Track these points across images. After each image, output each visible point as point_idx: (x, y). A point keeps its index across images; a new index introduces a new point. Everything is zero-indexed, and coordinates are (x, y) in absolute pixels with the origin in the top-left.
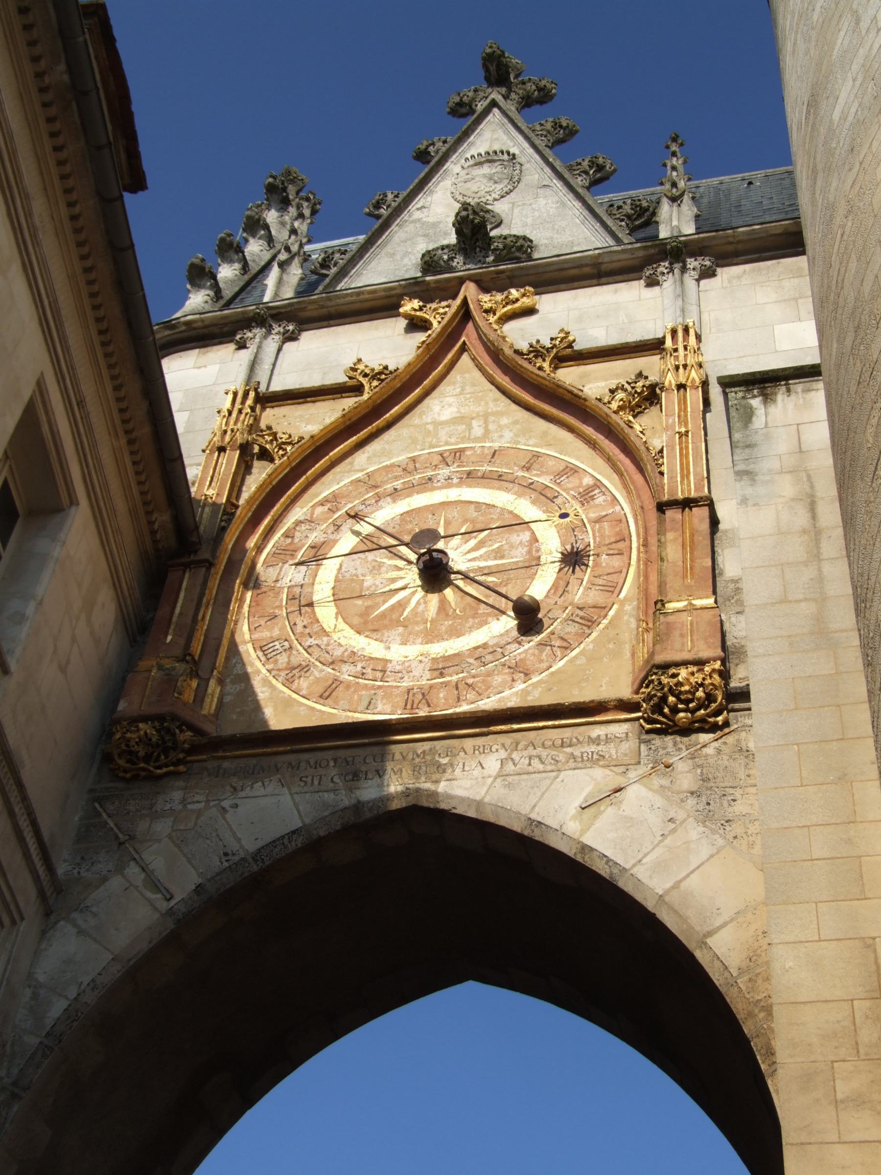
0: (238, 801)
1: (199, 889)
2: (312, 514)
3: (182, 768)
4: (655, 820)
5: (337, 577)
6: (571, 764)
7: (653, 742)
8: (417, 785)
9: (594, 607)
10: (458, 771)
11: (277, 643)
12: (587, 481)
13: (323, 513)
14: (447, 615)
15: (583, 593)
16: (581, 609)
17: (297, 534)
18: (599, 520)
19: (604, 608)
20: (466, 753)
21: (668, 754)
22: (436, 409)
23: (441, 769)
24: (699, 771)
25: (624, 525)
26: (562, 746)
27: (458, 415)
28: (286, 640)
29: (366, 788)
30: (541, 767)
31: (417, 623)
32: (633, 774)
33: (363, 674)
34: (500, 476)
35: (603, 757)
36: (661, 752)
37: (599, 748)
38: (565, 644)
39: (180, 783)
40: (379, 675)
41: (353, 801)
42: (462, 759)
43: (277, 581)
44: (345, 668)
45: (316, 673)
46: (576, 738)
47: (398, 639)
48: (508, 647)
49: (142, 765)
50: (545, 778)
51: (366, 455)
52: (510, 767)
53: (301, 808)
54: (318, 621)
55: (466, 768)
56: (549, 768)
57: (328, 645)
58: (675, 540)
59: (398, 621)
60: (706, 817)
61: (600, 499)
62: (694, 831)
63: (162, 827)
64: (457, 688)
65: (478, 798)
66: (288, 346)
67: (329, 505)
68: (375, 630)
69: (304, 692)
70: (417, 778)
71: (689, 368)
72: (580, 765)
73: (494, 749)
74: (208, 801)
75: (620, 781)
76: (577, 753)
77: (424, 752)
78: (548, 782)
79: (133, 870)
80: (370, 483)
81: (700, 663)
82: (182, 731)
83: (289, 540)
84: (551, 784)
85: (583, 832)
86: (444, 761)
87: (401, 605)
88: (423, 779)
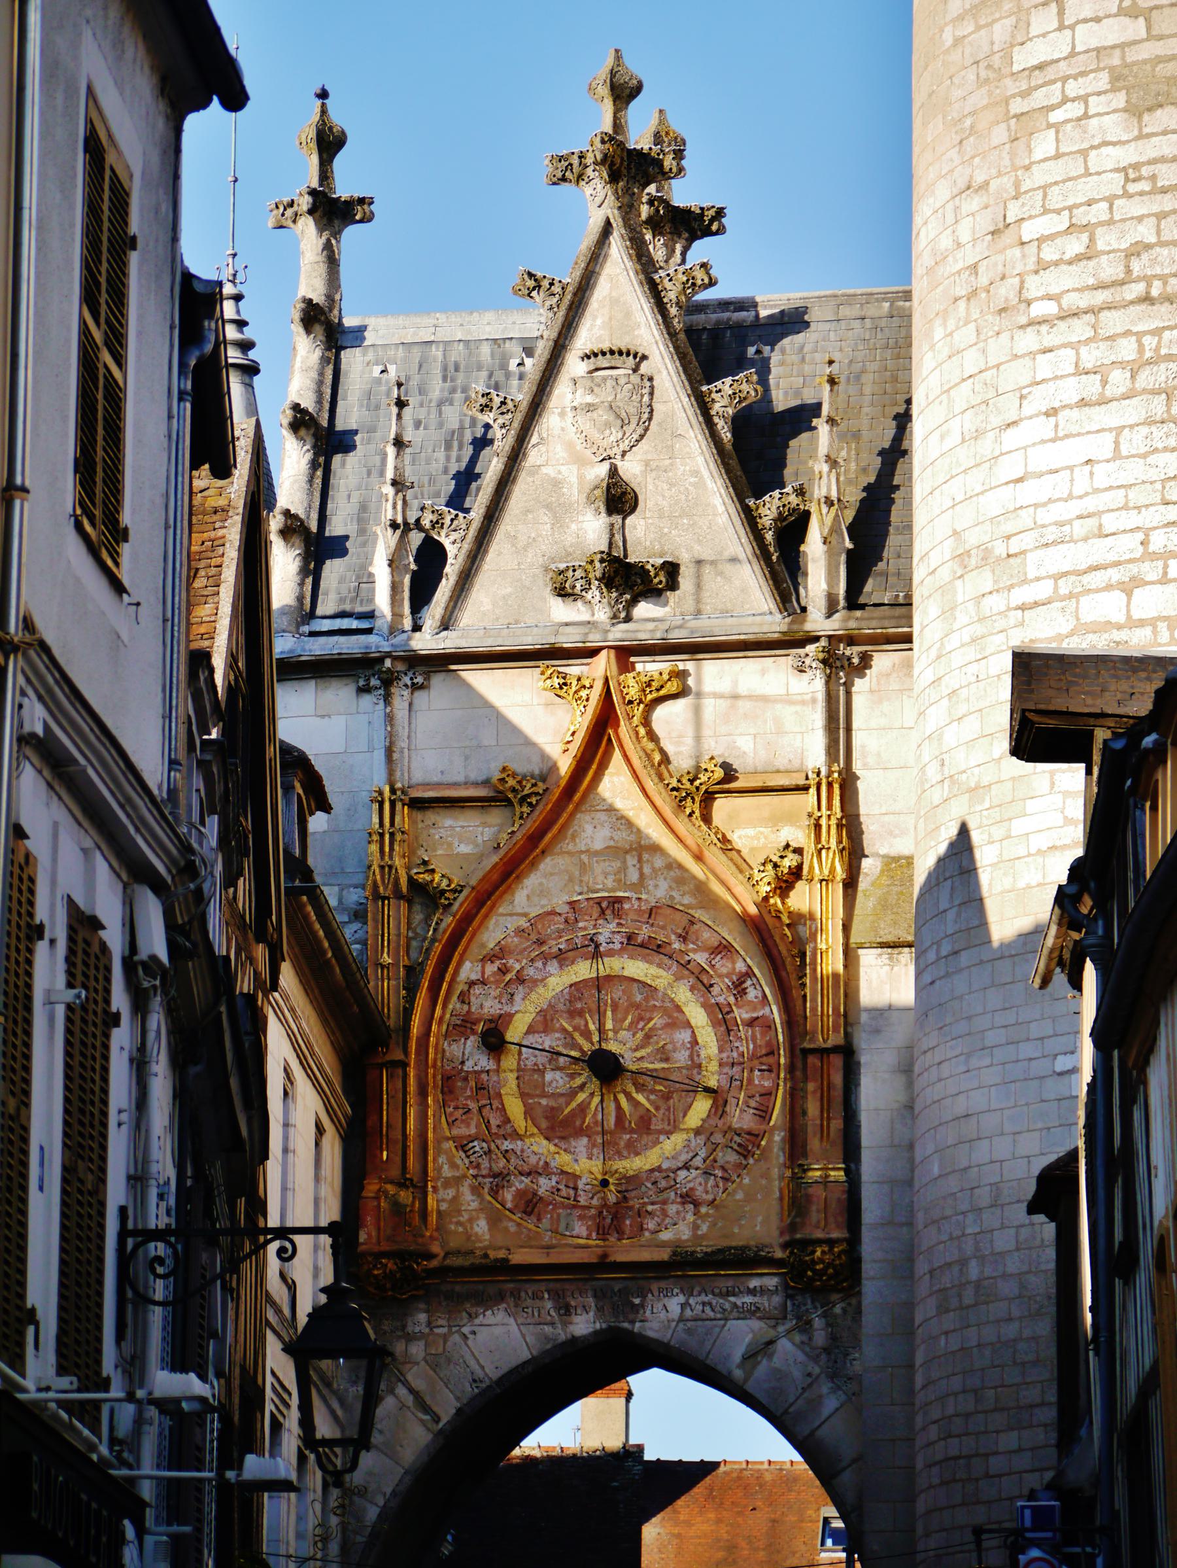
1: (459, 1411)
2: (483, 973)
3: (421, 1292)
4: (797, 1373)
6: (735, 1314)
9: (749, 1133)
10: (648, 1312)
12: (740, 966)
13: (494, 974)
15: (740, 1117)
17: (473, 999)
18: (751, 1023)
22: (589, 829)
23: (635, 1309)
27: (612, 843)
30: (712, 1314)
32: (781, 1329)
34: (659, 946)
37: (756, 1299)
39: (422, 1306)
40: (572, 1192)
43: (463, 1063)
44: (542, 1181)
58: (814, 1092)
59: (581, 1129)
60: (835, 1374)
61: (752, 994)
62: (825, 1387)
63: (417, 1350)
66: (417, 694)
67: (498, 963)
68: (562, 1138)
69: (509, 1205)
75: (772, 1333)
76: (739, 1303)
79: (401, 1391)
80: (534, 934)
81: (831, 1243)
83: (466, 1007)
85: (746, 1380)
86: (637, 1301)
87: (583, 1108)
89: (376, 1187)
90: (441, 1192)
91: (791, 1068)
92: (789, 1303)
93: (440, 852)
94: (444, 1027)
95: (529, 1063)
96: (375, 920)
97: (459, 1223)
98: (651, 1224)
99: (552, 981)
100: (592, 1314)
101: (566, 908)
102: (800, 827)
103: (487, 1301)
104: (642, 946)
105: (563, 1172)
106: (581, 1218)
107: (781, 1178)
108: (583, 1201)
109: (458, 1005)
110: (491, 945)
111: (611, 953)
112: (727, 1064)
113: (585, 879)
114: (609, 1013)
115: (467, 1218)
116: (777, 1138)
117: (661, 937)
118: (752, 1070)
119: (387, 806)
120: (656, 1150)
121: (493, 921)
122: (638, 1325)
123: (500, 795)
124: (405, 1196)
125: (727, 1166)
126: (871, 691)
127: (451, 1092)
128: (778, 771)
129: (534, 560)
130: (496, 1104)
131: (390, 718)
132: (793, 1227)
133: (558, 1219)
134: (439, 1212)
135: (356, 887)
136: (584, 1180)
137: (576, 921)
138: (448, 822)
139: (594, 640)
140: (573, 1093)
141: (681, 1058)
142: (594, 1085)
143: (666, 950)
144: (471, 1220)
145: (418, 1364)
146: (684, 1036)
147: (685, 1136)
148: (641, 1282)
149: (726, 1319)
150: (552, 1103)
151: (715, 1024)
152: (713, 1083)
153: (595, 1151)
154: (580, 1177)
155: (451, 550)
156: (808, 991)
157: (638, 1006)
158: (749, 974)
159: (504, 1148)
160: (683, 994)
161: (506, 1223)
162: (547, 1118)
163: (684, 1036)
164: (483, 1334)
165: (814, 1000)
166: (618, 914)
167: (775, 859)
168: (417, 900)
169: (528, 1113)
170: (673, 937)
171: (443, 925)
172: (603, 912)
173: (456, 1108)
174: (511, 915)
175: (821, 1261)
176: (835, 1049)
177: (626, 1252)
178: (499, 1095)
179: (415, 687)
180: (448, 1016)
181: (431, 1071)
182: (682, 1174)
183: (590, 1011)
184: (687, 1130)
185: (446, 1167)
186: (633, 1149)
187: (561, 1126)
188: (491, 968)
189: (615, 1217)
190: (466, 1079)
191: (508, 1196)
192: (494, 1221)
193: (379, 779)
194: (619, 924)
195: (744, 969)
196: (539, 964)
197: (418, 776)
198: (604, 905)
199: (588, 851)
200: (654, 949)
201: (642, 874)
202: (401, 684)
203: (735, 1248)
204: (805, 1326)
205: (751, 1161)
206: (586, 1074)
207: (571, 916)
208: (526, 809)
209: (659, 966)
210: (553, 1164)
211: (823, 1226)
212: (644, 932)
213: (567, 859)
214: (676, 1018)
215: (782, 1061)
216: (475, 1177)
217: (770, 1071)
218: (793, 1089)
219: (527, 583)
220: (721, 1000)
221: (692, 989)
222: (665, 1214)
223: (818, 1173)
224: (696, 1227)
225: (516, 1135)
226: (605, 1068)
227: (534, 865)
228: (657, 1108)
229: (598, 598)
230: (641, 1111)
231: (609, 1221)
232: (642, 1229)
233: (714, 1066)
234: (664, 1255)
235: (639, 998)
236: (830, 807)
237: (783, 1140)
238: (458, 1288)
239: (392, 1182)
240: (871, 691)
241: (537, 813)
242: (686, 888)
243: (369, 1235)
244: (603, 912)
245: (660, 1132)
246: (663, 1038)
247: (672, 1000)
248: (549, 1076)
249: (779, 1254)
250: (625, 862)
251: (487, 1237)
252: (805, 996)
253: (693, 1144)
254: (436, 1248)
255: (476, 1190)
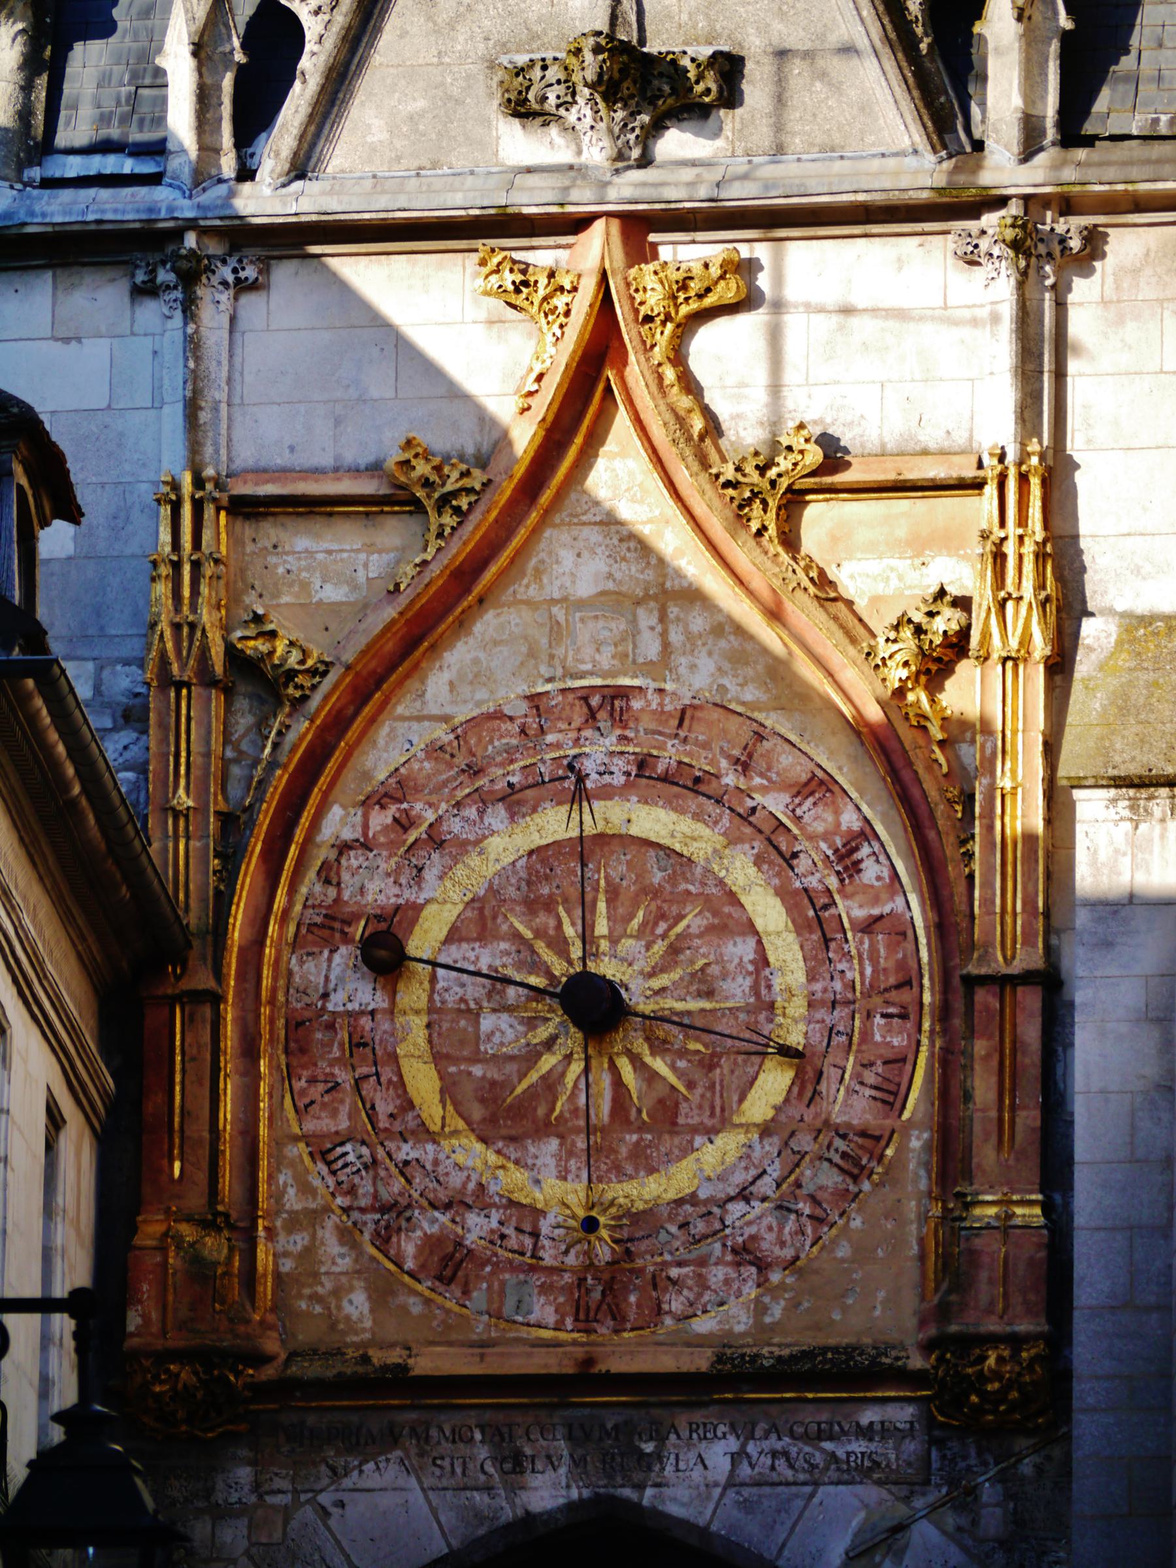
0: (346, 1497)
2: (366, 826)
5: (431, 999)
6: (833, 1474)
7: (950, 1444)
8: (612, 1490)
9: (863, 1134)
10: (669, 1469)
11: (348, 1147)
12: (850, 820)
13: (386, 829)
14: (628, 1122)
16: (844, 1137)
17: (346, 876)
18: (869, 926)
19: (878, 1139)
20: (679, 1437)
21: (969, 1468)
22: (567, 558)
23: (646, 1462)
24: (1011, 1505)
25: (910, 946)
26: (820, 1439)
27: (610, 586)
28: (363, 1143)
29: (536, 1489)
30: (789, 1474)
31: (577, 1131)
32: (919, 1503)
33: (503, 1237)
34: (697, 780)
35: (878, 1464)
36: (962, 1465)
37: (873, 1446)
38: (818, 1212)
39: (244, 1453)
40: (528, 1242)
41: (520, 1512)
42: (675, 1446)
43: (325, 996)
44: (473, 1219)
45: (425, 1225)
46: (839, 1424)
47: (552, 1162)
48: (729, 1206)
49: (184, 1428)
50: (797, 1496)
51: (446, 676)
52: (745, 1471)
53: (443, 1519)
54: (410, 1105)
55: (682, 1466)
56: (802, 1477)
57: (436, 1162)
58: (987, 1058)
59: (548, 1124)
61: (871, 872)
63: (234, 1535)
64: (655, 1287)
65: (701, 1522)
66: (246, 299)
67: (393, 809)
68: (513, 1139)
69: (410, 1264)
70: (611, 1477)
71: (1024, 606)
72: (846, 1477)
73: (719, 1434)
74: (296, 1492)
75: (902, 1511)
76: (841, 1453)
77: (616, 1427)
78: (800, 1503)
80: (463, 753)
81: (1016, 1341)
82: (238, 1374)
83: (332, 892)
84: (805, 1507)
86: (649, 1447)
87: (550, 1083)
88: (619, 1480)
89: (160, 1228)
90: (282, 1238)
91: (944, 1013)
92: (934, 1454)
93: (285, 599)
94: (292, 929)
95: (451, 999)
96: (163, 726)
97: (315, 1298)
98: (676, 1304)
99: (495, 844)
100: (563, 1470)
101: (523, 707)
102: (965, 557)
103: (368, 1444)
104: (665, 779)
105: (512, 1203)
106: (544, 1289)
107: (923, 1218)
108: (549, 1257)
109: (318, 888)
110: (382, 776)
111: (607, 793)
112: (823, 1003)
113: (560, 651)
114: (602, 906)
115: (332, 1287)
116: (915, 1144)
117: (702, 764)
118: (869, 1015)
119: (187, 511)
120: (688, 1163)
121: (384, 731)
122: (649, 1492)
123: (399, 496)
124: (214, 1246)
125: (820, 1195)
126: (1104, 302)
127: (303, 1051)
128: (925, 452)
129: (468, 45)
130: (387, 1073)
131: (193, 345)
132: (943, 1312)
133: (502, 1293)
134: (278, 1276)
135: (127, 663)
136: (551, 1219)
137: (542, 731)
138: (302, 543)
139: (581, 201)
140: (532, 1056)
141: (737, 990)
142: (573, 1039)
143: (712, 787)
144: (337, 1292)
145: (234, 1561)
146: (744, 949)
147: (742, 1138)
148: (656, 1412)
149: (816, 1484)
150: (494, 1074)
151: (801, 927)
152: (795, 1038)
153: (572, 1163)
154: (543, 1213)
155: (312, 26)
156: (977, 867)
157: (656, 892)
158: (867, 833)
159: (401, 1156)
160: (741, 870)
161: (402, 1299)
162: (482, 1101)
163: (744, 949)
164: (358, 1507)
165: (988, 884)
166: (620, 719)
167: (918, 617)
168: (242, 688)
169: (448, 1091)
170: (724, 763)
171: (291, 737)
172: (592, 715)
173: (312, 1081)
174: (420, 719)
175: (997, 1375)
176: (1027, 978)
177: (627, 1354)
178: (394, 1058)
179: (242, 287)
180: (298, 908)
181: (265, 1011)
182: (737, 1209)
183: (566, 901)
184: (747, 1127)
185: (291, 1191)
186: (645, 1162)
187: (509, 1118)
188: (380, 819)
189: (609, 1288)
190: (331, 1027)
191: (409, 1247)
192: (382, 1293)
193: (172, 461)
194: (623, 739)
195: (856, 825)
196: (471, 812)
197: (246, 455)
198: (595, 701)
199: (565, 599)
200: (687, 785)
201: (666, 645)
202: (215, 280)
203: (835, 1350)
204: (963, 1498)
205: (866, 1186)
206: (557, 1019)
207: (533, 723)
208: (449, 520)
209: (697, 817)
210: (493, 1188)
211: (1001, 1312)
212: (670, 754)
213: (526, 614)
214: (727, 916)
215: (927, 998)
216: (346, 1210)
217: (903, 1016)
218: (946, 1050)
219: (455, 91)
220: (813, 882)
221: (758, 861)
222: (703, 1284)
223: (992, 1211)
224: (760, 1309)
225: (423, 1133)
226: (594, 1008)
227: (462, 625)
228: (691, 1085)
229: (588, 121)
230: (660, 1090)
231: (597, 1295)
232: (659, 1311)
233: (798, 1007)
234: (701, 1361)
235: (657, 877)
236: (1022, 521)
237: (928, 1147)
238: (311, 1420)
239: (189, 1219)
240: (1104, 302)
241: (469, 527)
242: (750, 671)
243: (145, 1317)
244: (592, 715)
245: (694, 1130)
246: (702, 954)
247: (721, 882)
248: (487, 1023)
249: (917, 1362)
250: (634, 621)
251: (368, 1324)
252: (971, 877)
253: (757, 1153)
254: (271, 1344)
255: (347, 1236)
